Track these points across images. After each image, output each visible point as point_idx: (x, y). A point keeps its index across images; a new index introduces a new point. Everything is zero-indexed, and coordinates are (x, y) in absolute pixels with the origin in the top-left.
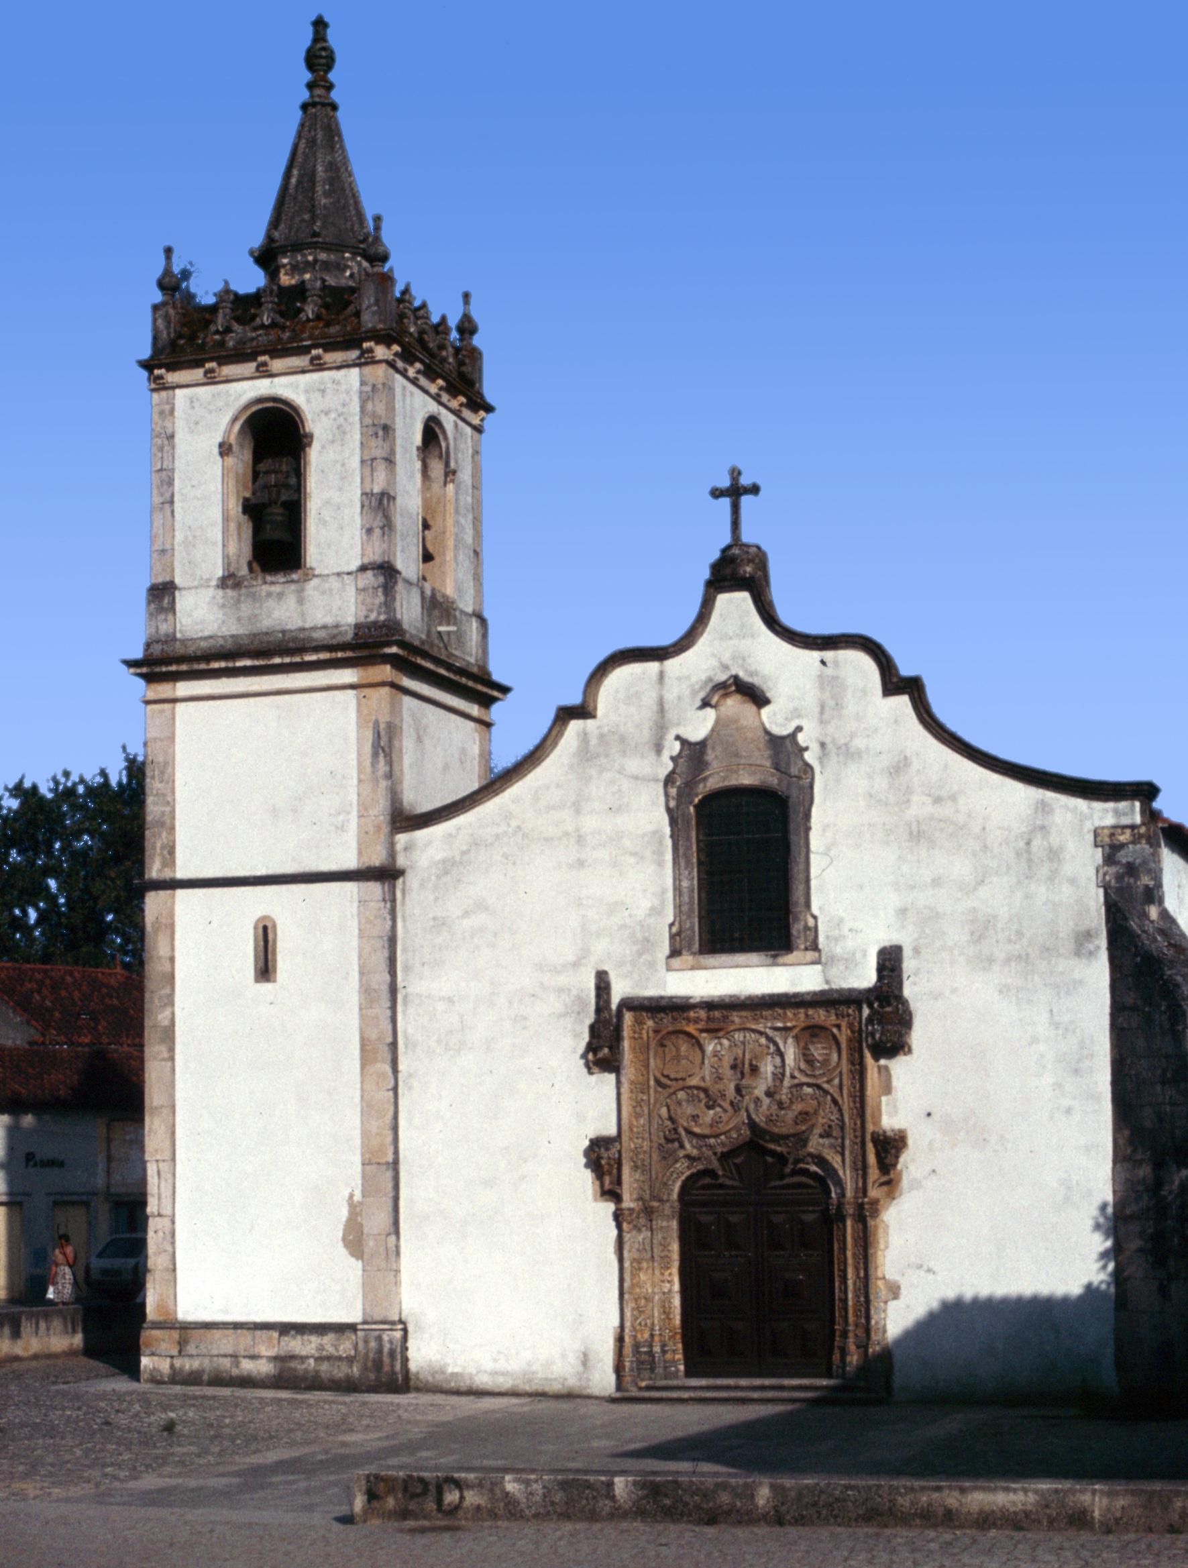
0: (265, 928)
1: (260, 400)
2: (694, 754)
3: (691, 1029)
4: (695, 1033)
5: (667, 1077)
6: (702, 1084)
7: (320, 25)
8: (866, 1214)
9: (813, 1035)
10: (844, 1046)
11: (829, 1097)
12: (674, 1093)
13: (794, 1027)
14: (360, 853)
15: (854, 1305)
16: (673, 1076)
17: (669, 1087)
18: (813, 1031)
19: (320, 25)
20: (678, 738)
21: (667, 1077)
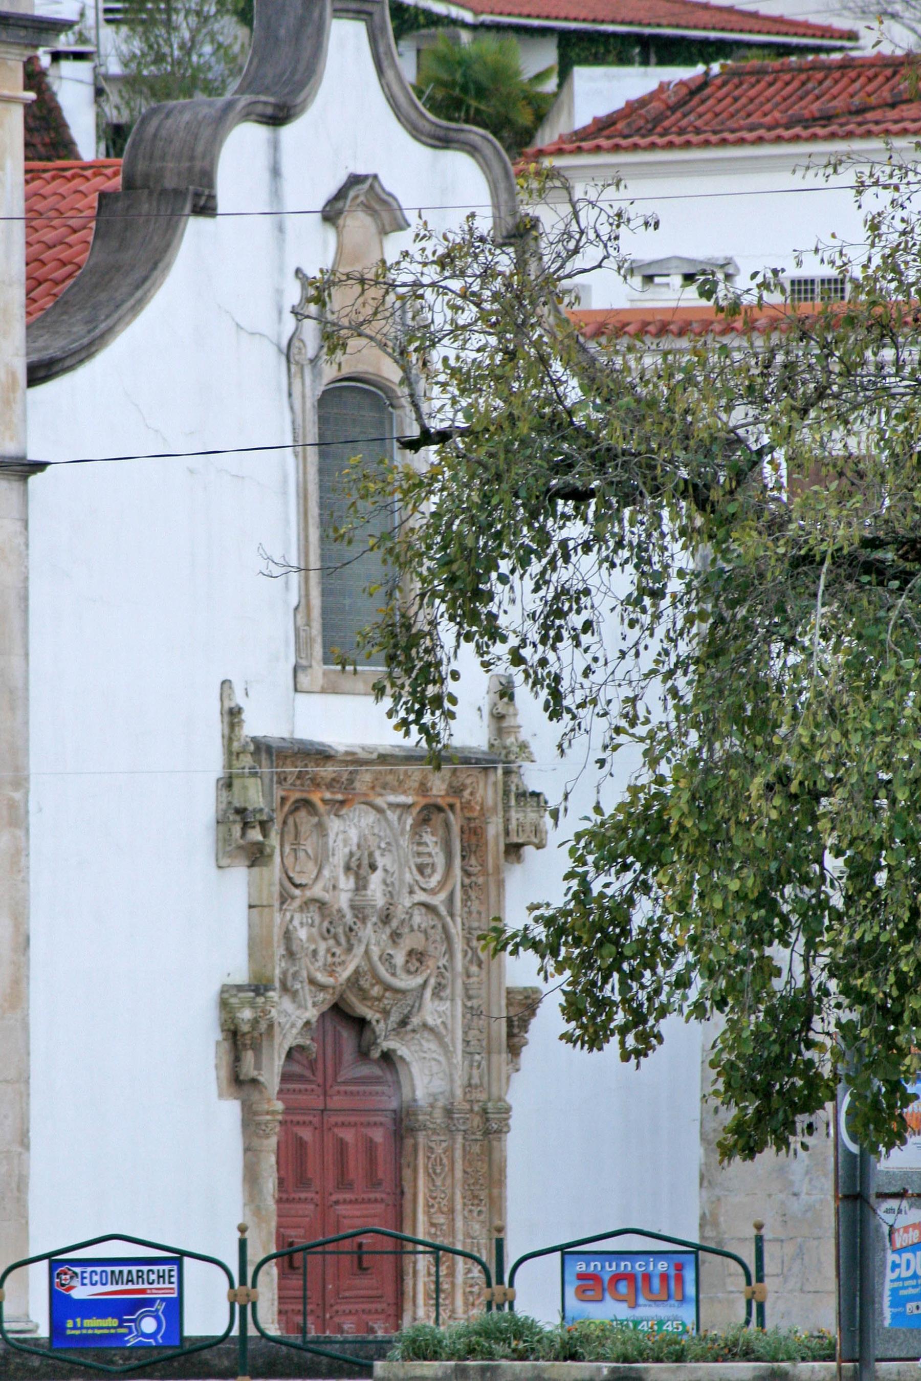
21: (290, 879)
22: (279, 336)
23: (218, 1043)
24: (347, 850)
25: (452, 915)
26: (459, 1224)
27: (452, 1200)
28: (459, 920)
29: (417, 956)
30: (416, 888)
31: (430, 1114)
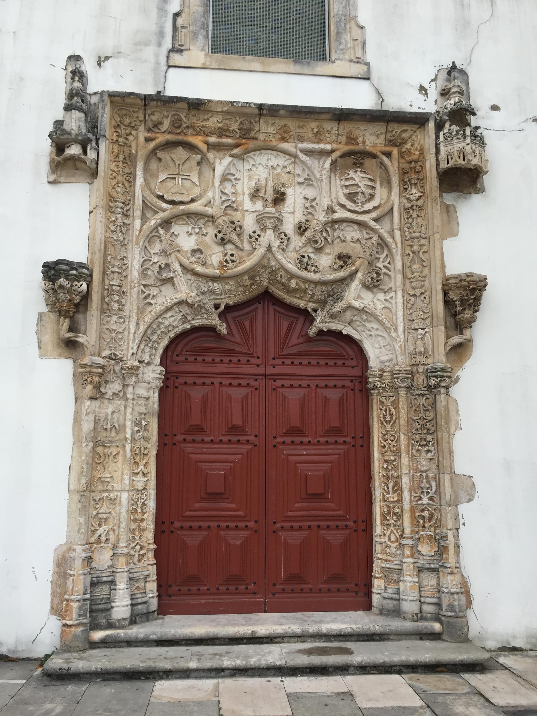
3: (197, 141)
4: (204, 148)
5: (161, 198)
6: (209, 210)
8: (432, 385)
9: (358, 165)
13: (333, 151)
15: (413, 510)
16: (168, 197)
17: (164, 210)
18: (357, 158)
23: (41, 316)
24: (253, 184)
26: (405, 460)
27: (398, 441)
28: (397, 233)
29: (344, 259)
31: (380, 377)
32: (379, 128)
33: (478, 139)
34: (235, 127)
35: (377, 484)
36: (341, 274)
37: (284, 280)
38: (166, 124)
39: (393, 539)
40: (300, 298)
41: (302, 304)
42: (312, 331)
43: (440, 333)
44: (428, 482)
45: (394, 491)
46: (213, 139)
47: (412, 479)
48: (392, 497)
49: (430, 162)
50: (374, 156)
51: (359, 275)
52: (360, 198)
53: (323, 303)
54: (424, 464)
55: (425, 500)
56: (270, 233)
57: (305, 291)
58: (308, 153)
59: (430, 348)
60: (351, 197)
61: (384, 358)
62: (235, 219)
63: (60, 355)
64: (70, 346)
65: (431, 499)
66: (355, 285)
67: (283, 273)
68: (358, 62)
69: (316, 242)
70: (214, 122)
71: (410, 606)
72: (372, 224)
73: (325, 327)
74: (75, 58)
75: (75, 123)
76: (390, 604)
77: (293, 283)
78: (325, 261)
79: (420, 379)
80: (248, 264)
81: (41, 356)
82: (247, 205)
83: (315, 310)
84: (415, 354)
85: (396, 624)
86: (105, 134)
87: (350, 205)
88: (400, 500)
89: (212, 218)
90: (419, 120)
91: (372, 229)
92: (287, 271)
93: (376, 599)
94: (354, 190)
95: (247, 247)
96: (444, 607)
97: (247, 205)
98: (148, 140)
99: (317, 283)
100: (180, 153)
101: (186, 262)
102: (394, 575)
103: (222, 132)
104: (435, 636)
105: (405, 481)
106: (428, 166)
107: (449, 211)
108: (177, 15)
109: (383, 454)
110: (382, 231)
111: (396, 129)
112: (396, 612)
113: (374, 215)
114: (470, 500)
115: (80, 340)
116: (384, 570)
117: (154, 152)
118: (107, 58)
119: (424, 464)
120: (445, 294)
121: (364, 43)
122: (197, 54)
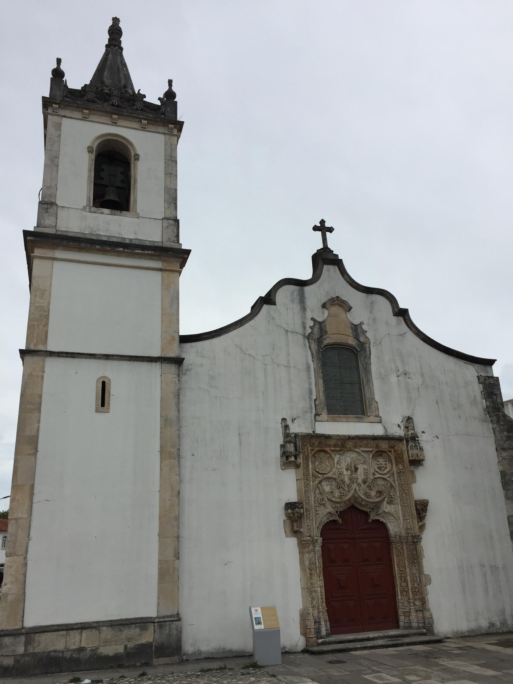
0: (104, 383)
1: (110, 134)
2: (321, 326)
3: (327, 449)
4: (330, 452)
5: (318, 472)
7: (116, 20)
8: (414, 541)
10: (394, 461)
11: (389, 484)
12: (320, 482)
14: (163, 350)
15: (412, 588)
17: (319, 477)
19: (116, 20)
20: (312, 319)
21: (318, 472)
22: (305, 333)
23: (284, 521)
24: (346, 464)
25: (394, 481)
26: (408, 570)
27: (405, 563)
28: (397, 482)
29: (380, 493)
30: (376, 473)
31: (395, 538)
32: (386, 442)
33: (421, 449)
34: (340, 443)
35: (397, 579)
36: (380, 499)
37: (360, 501)
38: (316, 444)
39: (405, 600)
40: (365, 508)
41: (366, 510)
42: (370, 521)
43: (416, 521)
44: (416, 578)
45: (404, 582)
46: (333, 449)
47: (411, 577)
48: (404, 584)
49: (405, 456)
50: (385, 452)
51: (386, 499)
52: (383, 468)
53: (373, 509)
54: (414, 571)
55: (416, 585)
56: (355, 484)
57: (367, 505)
58: (363, 451)
59: (412, 527)
60: (379, 468)
61: (396, 531)
62: (343, 479)
63: (292, 536)
64: (295, 533)
65: (418, 584)
66: (385, 503)
67: (360, 499)
68: (377, 416)
69: (370, 487)
70: (332, 442)
71: (415, 625)
72: (388, 479)
73: (374, 518)
74: (284, 420)
75: (291, 448)
76: (407, 625)
77: (363, 503)
78: (373, 493)
79: (410, 539)
80: (348, 497)
81: (287, 536)
82: (345, 472)
83: (370, 512)
84: (407, 529)
85: (412, 631)
86: (299, 450)
87: (379, 471)
88: (407, 585)
89: (335, 479)
90: (400, 439)
91: (387, 480)
92: (361, 498)
93: (401, 624)
94: (380, 466)
95: (346, 489)
96: (426, 623)
97: (345, 472)
98: (312, 450)
99: (371, 503)
100: (322, 453)
101: (329, 497)
102: (408, 614)
103: (335, 446)
104: (424, 634)
105: (408, 578)
106: (405, 457)
107: (413, 473)
108: (315, 400)
109: (399, 568)
110: (392, 482)
111: (392, 442)
112: (410, 627)
113: (388, 475)
114: (430, 584)
115: (301, 530)
116: (404, 613)
117: (314, 455)
118: (295, 419)
119: (414, 571)
120: (416, 506)
121: (378, 409)
122: (324, 416)
